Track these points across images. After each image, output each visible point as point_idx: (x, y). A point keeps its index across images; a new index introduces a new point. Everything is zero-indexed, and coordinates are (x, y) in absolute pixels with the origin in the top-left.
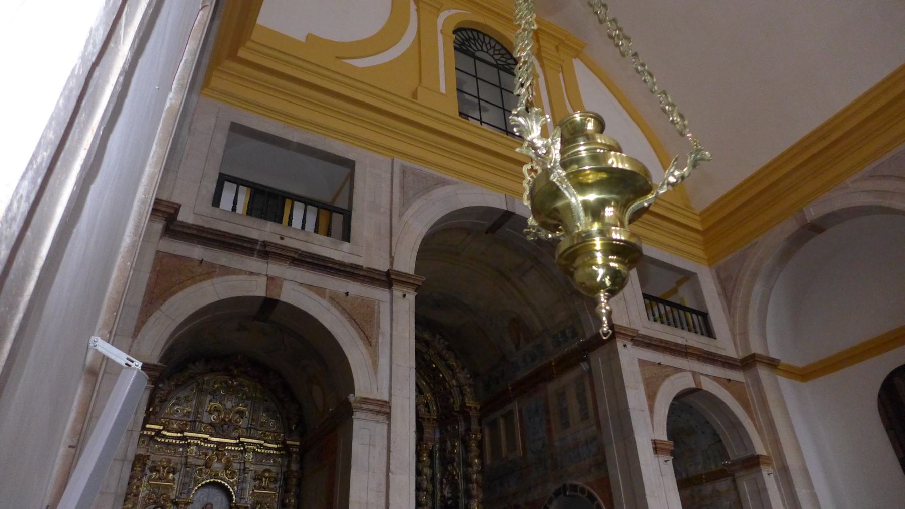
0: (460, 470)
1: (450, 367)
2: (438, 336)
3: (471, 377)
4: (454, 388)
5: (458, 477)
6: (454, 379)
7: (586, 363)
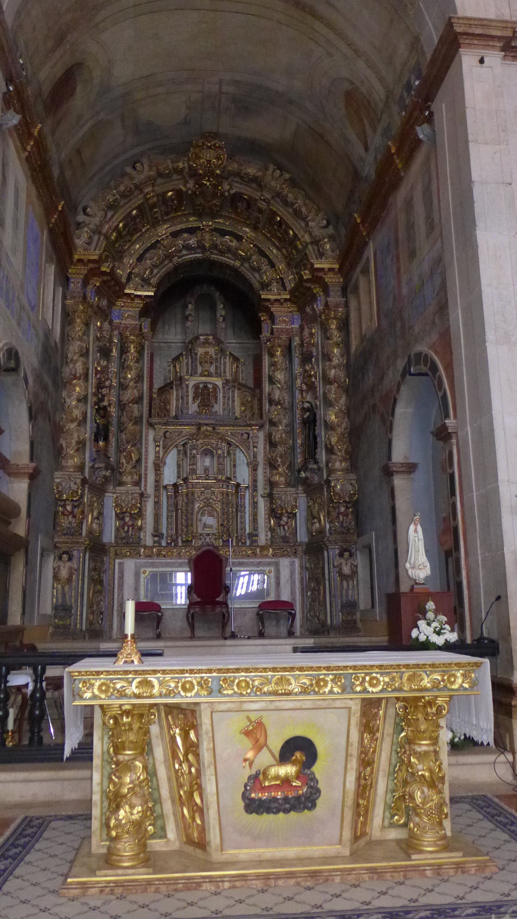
0: (318, 367)
1: (297, 214)
2: (271, 167)
3: (328, 223)
4: (310, 247)
5: (316, 379)
6: (305, 232)
7: (425, 126)
